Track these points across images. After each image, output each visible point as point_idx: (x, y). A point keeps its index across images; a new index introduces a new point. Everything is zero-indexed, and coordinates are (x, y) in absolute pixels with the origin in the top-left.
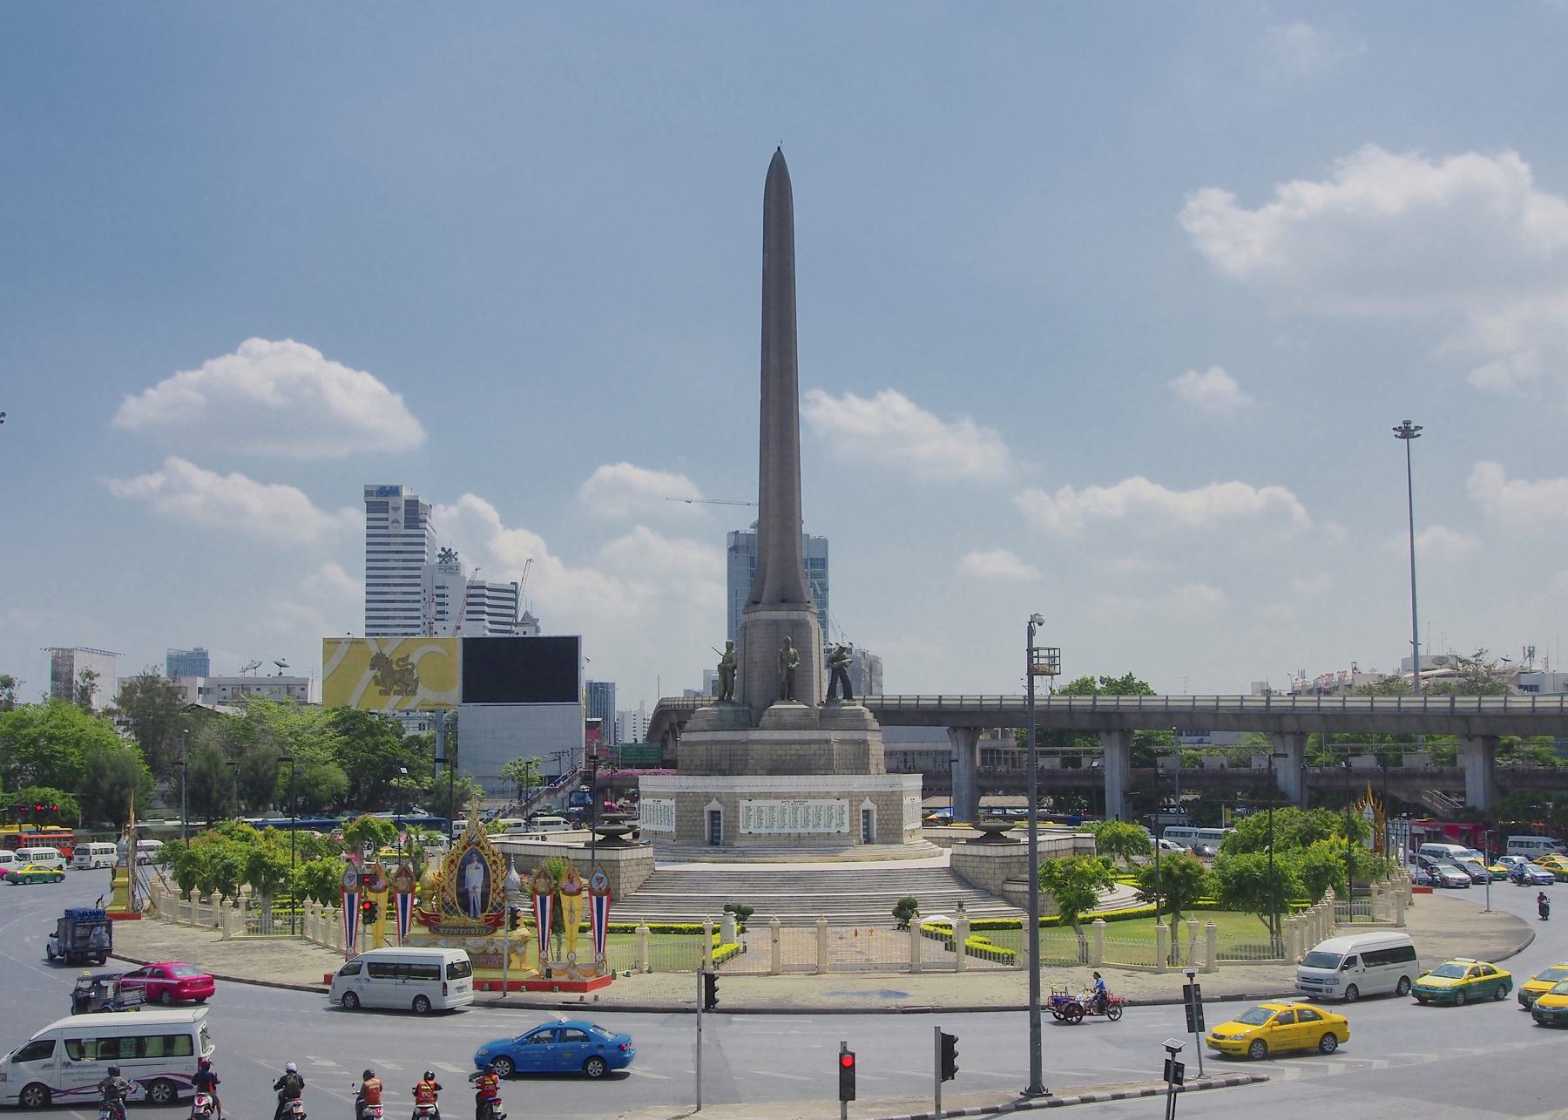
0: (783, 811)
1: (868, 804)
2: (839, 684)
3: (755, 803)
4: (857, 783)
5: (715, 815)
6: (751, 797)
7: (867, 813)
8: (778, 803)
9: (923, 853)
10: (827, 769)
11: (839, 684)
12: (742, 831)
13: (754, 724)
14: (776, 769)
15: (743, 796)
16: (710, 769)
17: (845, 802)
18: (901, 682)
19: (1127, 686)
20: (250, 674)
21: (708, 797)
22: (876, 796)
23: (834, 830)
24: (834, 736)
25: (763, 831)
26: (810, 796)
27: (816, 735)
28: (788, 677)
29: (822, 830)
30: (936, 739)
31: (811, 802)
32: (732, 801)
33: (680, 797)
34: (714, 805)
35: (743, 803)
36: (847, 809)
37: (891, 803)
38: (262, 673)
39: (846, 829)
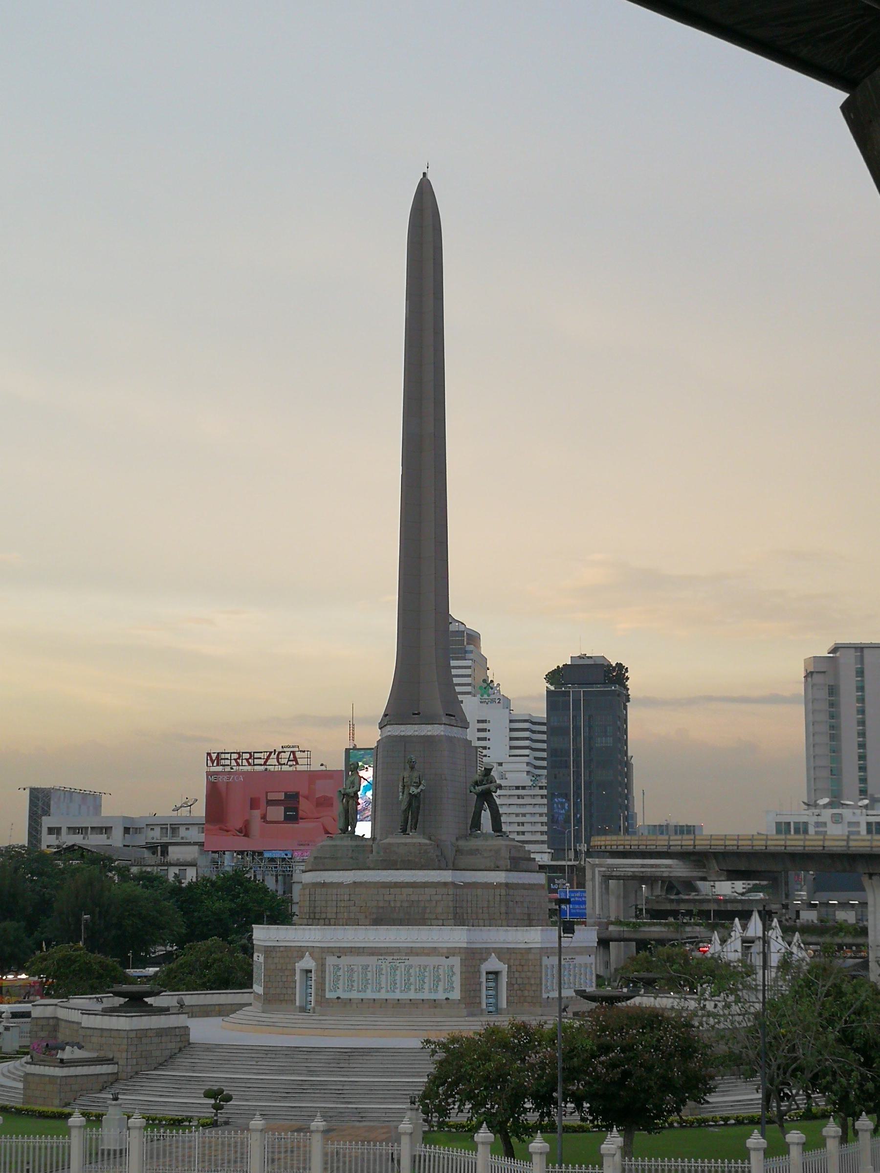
0: (379, 972)
1: (493, 963)
2: (486, 817)
3: (345, 961)
6: (340, 952)
7: (497, 973)
8: (372, 961)
11: (486, 817)
12: (328, 995)
15: (330, 951)
17: (456, 961)
20: (184, 812)
21: (300, 952)
22: (503, 954)
23: (441, 996)
25: (354, 995)
26: (412, 952)
28: (410, 805)
29: (426, 995)
31: (414, 960)
32: (321, 953)
34: (308, 962)
35: (331, 960)
36: (457, 969)
39: (456, 995)
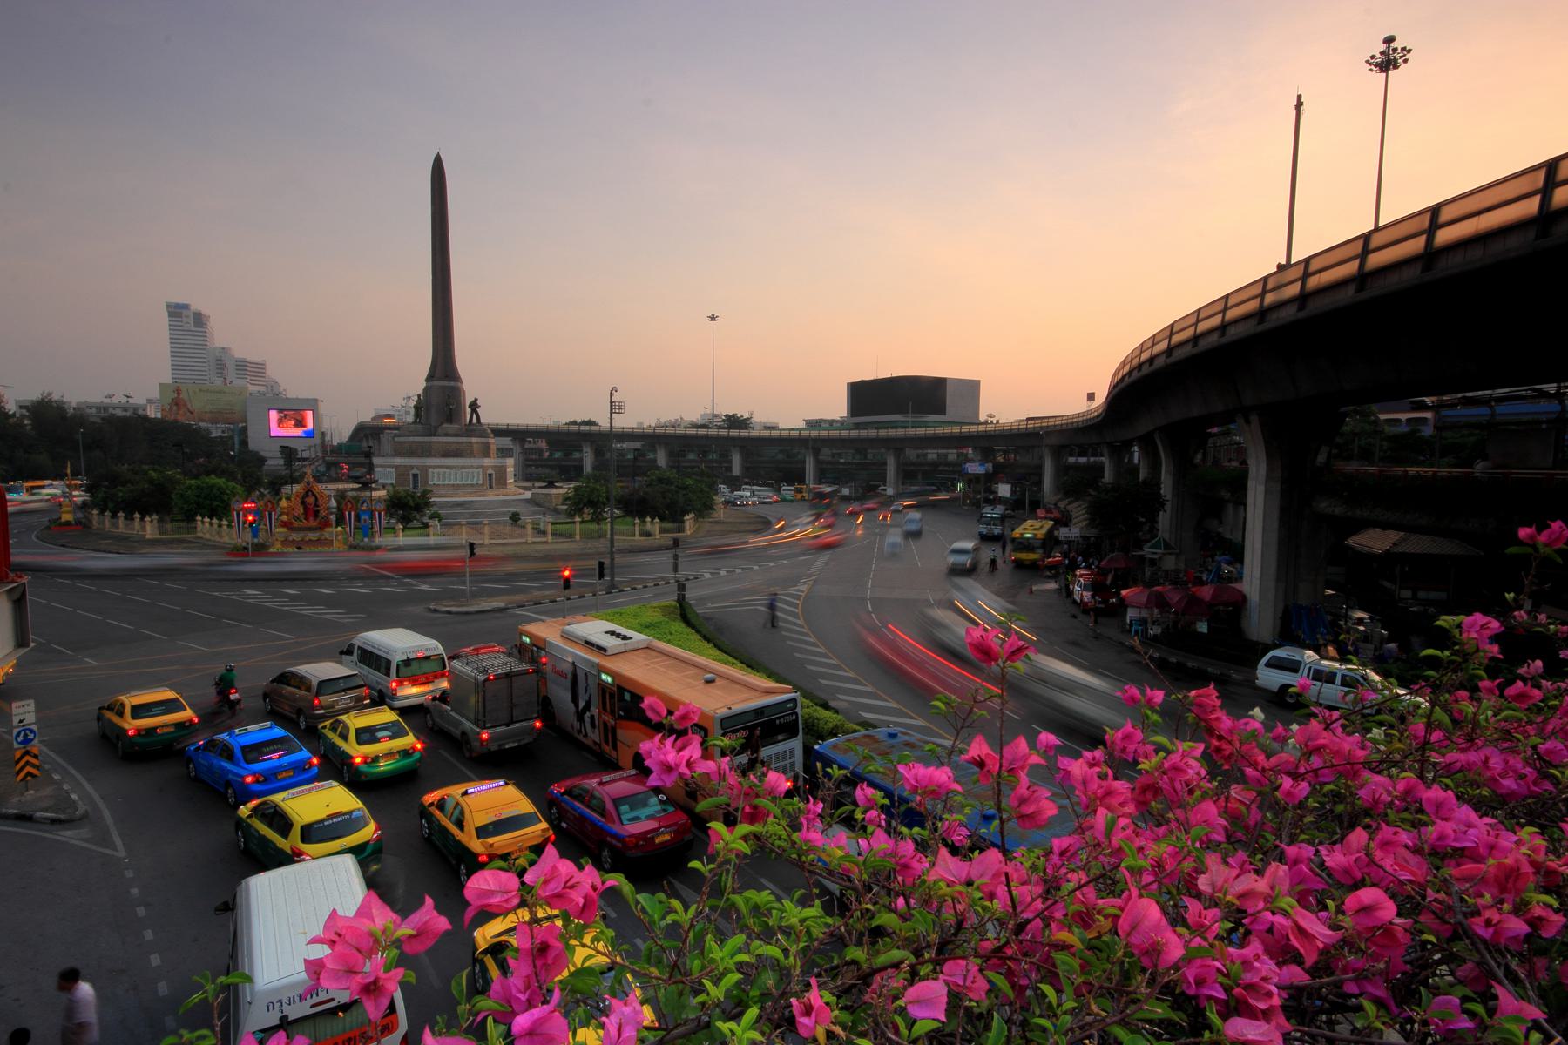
4: (487, 462)
5: (415, 476)
9: (515, 492)
10: (471, 455)
13: (433, 432)
14: (446, 455)
16: (412, 454)
18: (489, 416)
19: (590, 423)
21: (412, 467)
22: (494, 467)
24: (474, 440)
27: (464, 439)
30: (506, 442)
32: (425, 469)
33: (397, 467)
34: (415, 471)
37: (501, 471)
38: (115, 401)
